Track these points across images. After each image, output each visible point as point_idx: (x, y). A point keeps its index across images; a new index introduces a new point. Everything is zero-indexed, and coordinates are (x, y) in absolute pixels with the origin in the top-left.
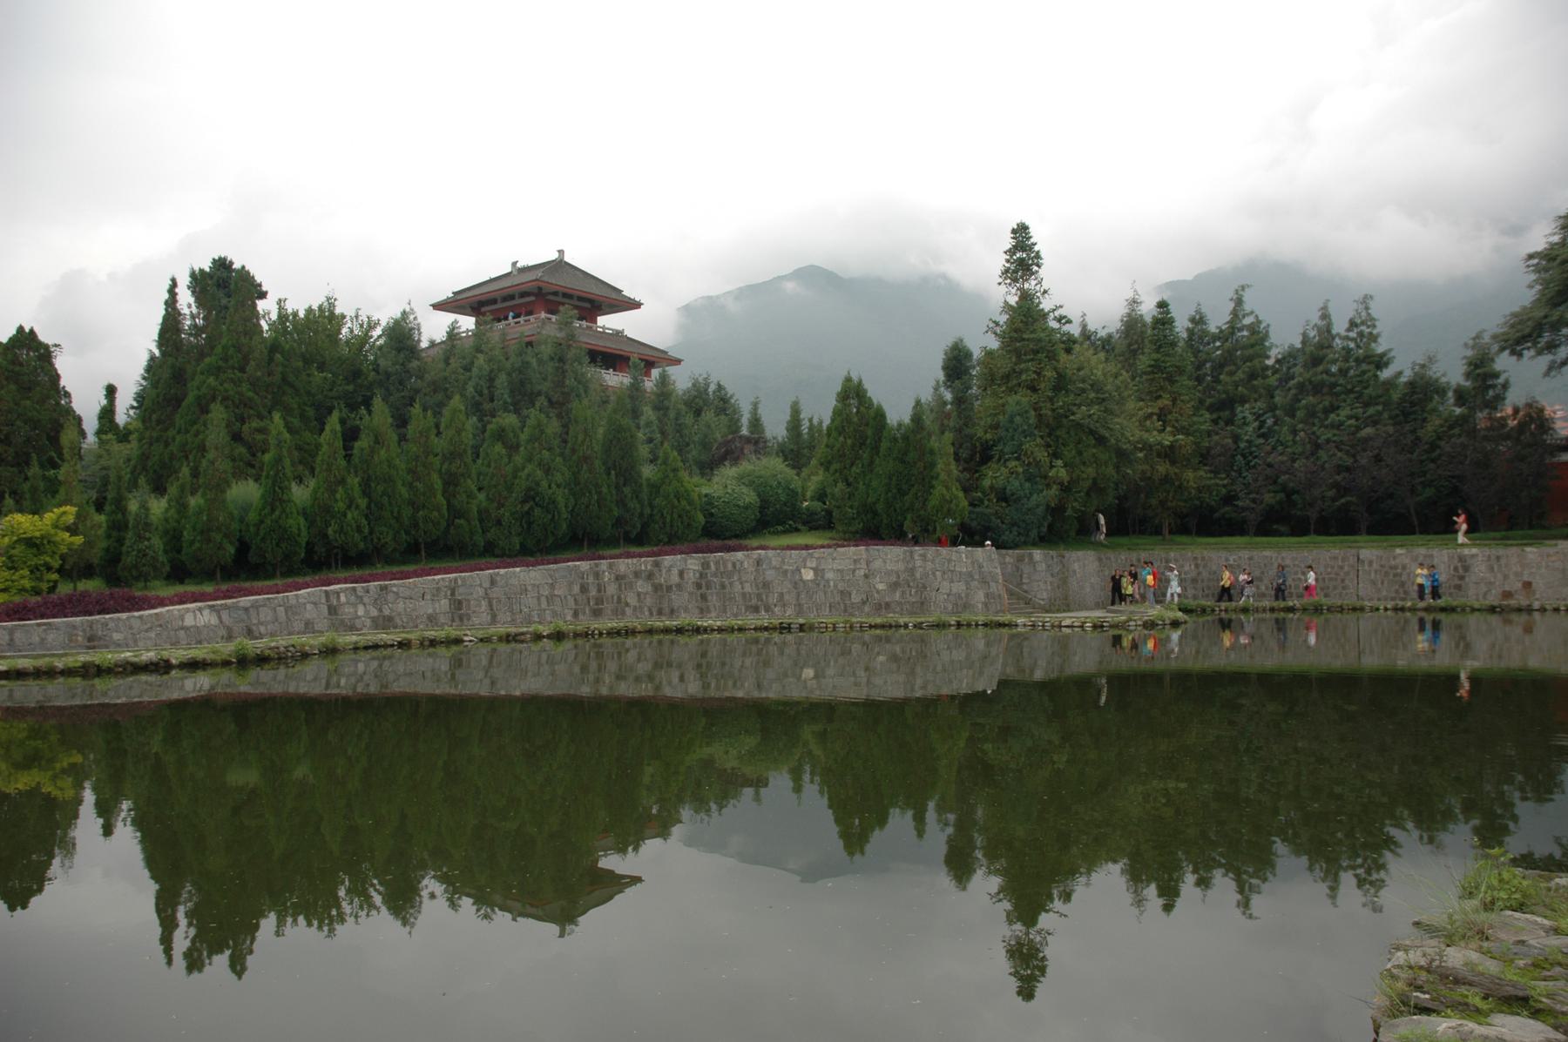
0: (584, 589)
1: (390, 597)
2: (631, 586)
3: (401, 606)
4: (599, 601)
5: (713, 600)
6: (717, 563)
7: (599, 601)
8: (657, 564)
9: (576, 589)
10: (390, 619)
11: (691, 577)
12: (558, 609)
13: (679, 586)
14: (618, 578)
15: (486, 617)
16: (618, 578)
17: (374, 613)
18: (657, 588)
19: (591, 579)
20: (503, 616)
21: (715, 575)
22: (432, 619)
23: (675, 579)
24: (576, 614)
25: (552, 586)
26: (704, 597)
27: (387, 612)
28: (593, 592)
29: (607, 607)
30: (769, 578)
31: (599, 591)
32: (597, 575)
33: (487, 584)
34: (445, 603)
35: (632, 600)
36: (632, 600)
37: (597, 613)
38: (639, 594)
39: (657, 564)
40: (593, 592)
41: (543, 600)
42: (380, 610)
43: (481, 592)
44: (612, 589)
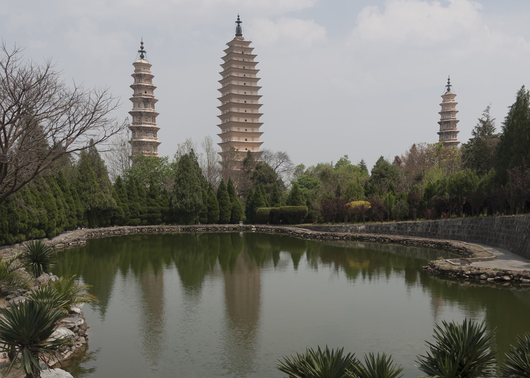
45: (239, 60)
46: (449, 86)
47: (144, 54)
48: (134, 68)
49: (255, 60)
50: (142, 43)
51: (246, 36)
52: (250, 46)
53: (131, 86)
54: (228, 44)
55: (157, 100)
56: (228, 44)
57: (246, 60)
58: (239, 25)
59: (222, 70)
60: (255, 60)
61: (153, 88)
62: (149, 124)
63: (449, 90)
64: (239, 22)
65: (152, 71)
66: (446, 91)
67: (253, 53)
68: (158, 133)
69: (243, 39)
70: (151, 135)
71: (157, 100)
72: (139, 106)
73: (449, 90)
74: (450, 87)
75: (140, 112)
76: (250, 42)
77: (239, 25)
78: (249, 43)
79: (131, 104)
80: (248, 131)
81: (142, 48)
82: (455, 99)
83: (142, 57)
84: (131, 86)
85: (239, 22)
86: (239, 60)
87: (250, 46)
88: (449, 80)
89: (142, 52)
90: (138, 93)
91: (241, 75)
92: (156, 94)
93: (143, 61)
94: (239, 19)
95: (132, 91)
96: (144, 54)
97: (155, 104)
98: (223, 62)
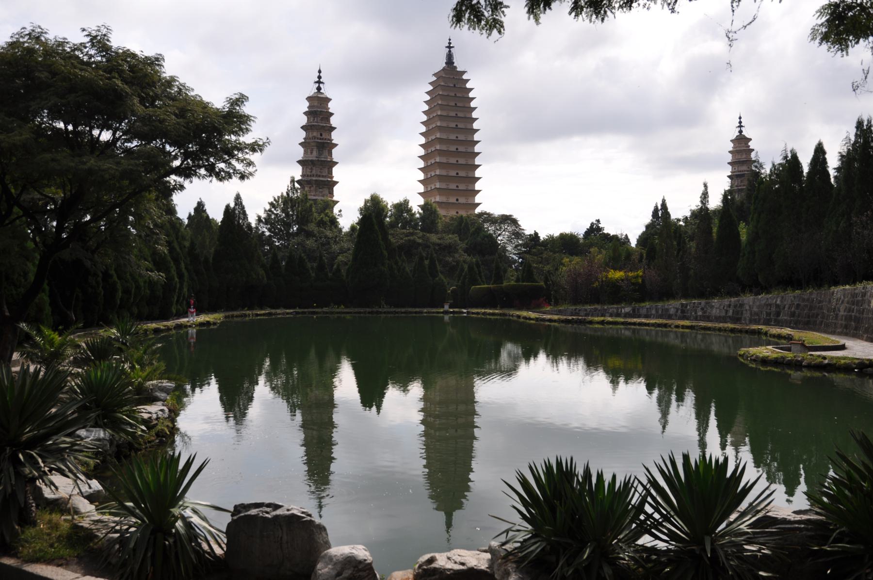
34: (730, 313)
42: (705, 312)
46: (740, 126)
47: (321, 85)
48: (307, 104)
50: (320, 72)
52: (465, 77)
53: (302, 128)
54: (435, 75)
55: (336, 145)
56: (435, 75)
58: (450, 51)
62: (323, 176)
63: (741, 132)
64: (449, 47)
65: (332, 107)
67: (468, 86)
69: (456, 67)
71: (336, 145)
72: (312, 153)
73: (741, 132)
74: (743, 129)
75: (312, 161)
76: (464, 72)
77: (450, 51)
78: (464, 72)
79: (301, 150)
80: (460, 188)
81: (319, 77)
82: (750, 144)
83: (319, 89)
84: (302, 128)
85: (449, 47)
87: (465, 77)
88: (740, 118)
89: (319, 82)
90: (311, 136)
91: (453, 114)
94: (450, 43)
96: (321, 85)
97: (334, 151)
98: (428, 98)
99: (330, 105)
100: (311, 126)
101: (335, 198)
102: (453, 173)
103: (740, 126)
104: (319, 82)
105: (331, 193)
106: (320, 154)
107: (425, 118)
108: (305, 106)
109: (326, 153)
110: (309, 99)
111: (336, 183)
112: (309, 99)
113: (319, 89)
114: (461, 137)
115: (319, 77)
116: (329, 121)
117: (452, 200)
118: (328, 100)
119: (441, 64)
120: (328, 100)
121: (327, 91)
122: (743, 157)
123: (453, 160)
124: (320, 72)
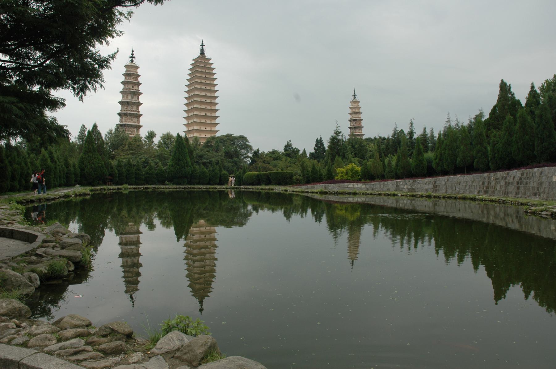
0: (483, 183)
1: (416, 183)
2: (500, 182)
3: (419, 186)
4: (488, 188)
5: (522, 189)
6: (527, 173)
7: (488, 188)
8: (508, 174)
9: (481, 183)
10: (414, 189)
11: (517, 179)
12: (472, 190)
13: (512, 183)
14: (496, 179)
15: (444, 191)
16: (496, 179)
17: (410, 187)
18: (506, 183)
19: (487, 179)
20: (450, 191)
21: (525, 179)
22: (427, 190)
23: (511, 180)
24: (479, 193)
25: (473, 182)
26: (518, 188)
27: (413, 188)
28: (486, 184)
29: (490, 190)
30: (543, 180)
31: (488, 184)
32: (489, 178)
33: (446, 181)
34: (431, 186)
35: (498, 188)
36: (498, 188)
37: (486, 192)
38: (501, 186)
39: (508, 174)
40: (486, 184)
41: (468, 187)
43: (444, 183)
44: (493, 183)
45: (202, 71)
46: (355, 95)
48: (125, 69)
49: (214, 72)
50: (133, 51)
51: (207, 54)
52: (210, 62)
54: (193, 60)
55: (141, 93)
57: (207, 71)
59: (189, 77)
60: (214, 72)
61: (139, 84)
63: (355, 98)
64: (202, 45)
65: (139, 71)
66: (353, 98)
67: (212, 66)
68: (140, 118)
69: (205, 56)
70: (135, 120)
71: (141, 93)
73: (355, 98)
75: (127, 102)
81: (132, 54)
83: (132, 61)
85: (202, 45)
86: (202, 71)
87: (210, 62)
89: (132, 57)
90: (127, 88)
91: (204, 81)
92: (141, 88)
93: (133, 64)
95: (122, 86)
99: (138, 70)
100: (127, 82)
101: (141, 124)
102: (203, 114)
103: (355, 95)
104: (132, 57)
105: (138, 121)
106: (132, 98)
107: (188, 83)
108: (124, 70)
109: (135, 98)
110: (126, 66)
111: (142, 115)
112: (126, 66)
113: (132, 61)
114: (208, 94)
115: (132, 54)
116: (137, 79)
117: (203, 128)
118: (138, 67)
119: (197, 54)
120: (138, 67)
121: (136, 62)
122: (356, 111)
123: (203, 107)
124: (133, 51)
